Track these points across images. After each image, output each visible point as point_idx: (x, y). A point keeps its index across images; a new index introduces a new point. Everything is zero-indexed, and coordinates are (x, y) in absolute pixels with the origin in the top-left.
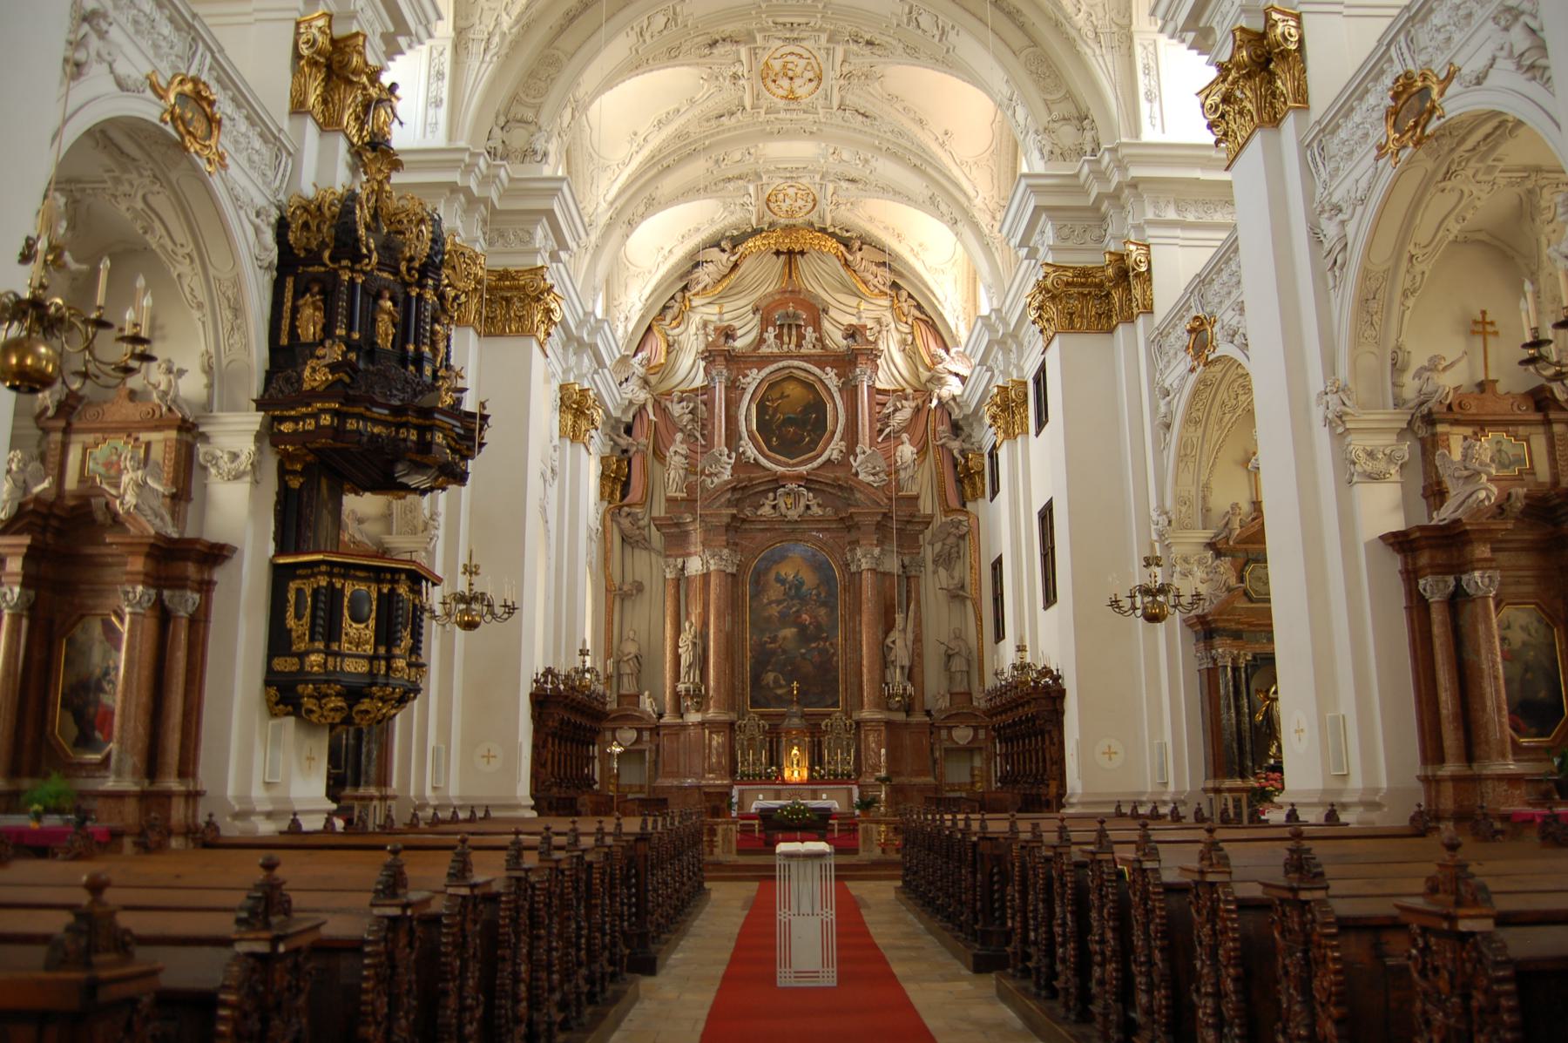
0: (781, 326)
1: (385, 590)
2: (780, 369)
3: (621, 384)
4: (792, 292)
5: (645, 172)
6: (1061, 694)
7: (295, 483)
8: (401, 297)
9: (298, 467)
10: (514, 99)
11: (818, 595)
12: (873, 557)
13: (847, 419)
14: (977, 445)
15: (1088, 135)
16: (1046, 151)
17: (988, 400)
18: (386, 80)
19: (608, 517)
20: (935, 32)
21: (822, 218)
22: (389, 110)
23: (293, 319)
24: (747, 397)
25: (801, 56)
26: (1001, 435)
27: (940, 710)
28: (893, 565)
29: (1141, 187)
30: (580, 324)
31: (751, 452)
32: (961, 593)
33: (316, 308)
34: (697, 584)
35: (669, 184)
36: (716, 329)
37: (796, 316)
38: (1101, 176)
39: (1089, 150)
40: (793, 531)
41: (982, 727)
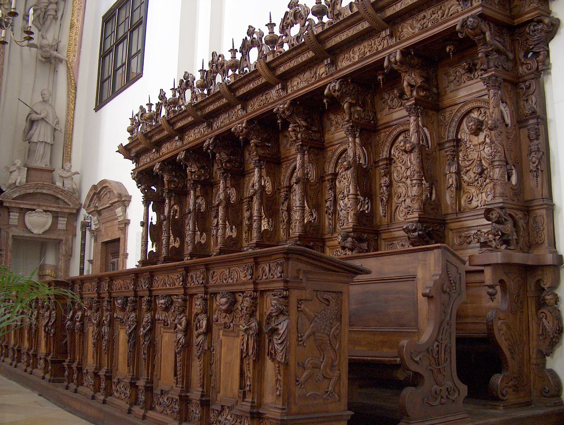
27: (14, 186)
41: (63, 214)
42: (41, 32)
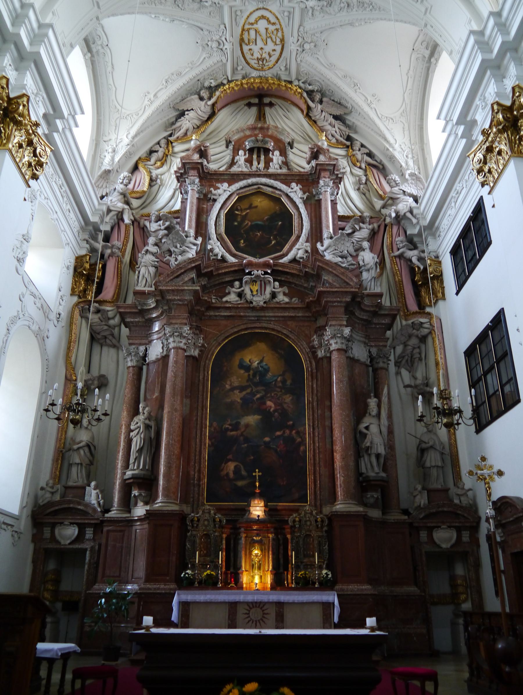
2: (249, 186)
4: (262, 129)
11: (284, 382)
12: (343, 337)
14: (433, 255)
19: (77, 312)
21: (287, 69)
24: (217, 206)
31: (219, 250)
32: (428, 389)
34: (153, 369)
40: (259, 319)
42: (411, 373)
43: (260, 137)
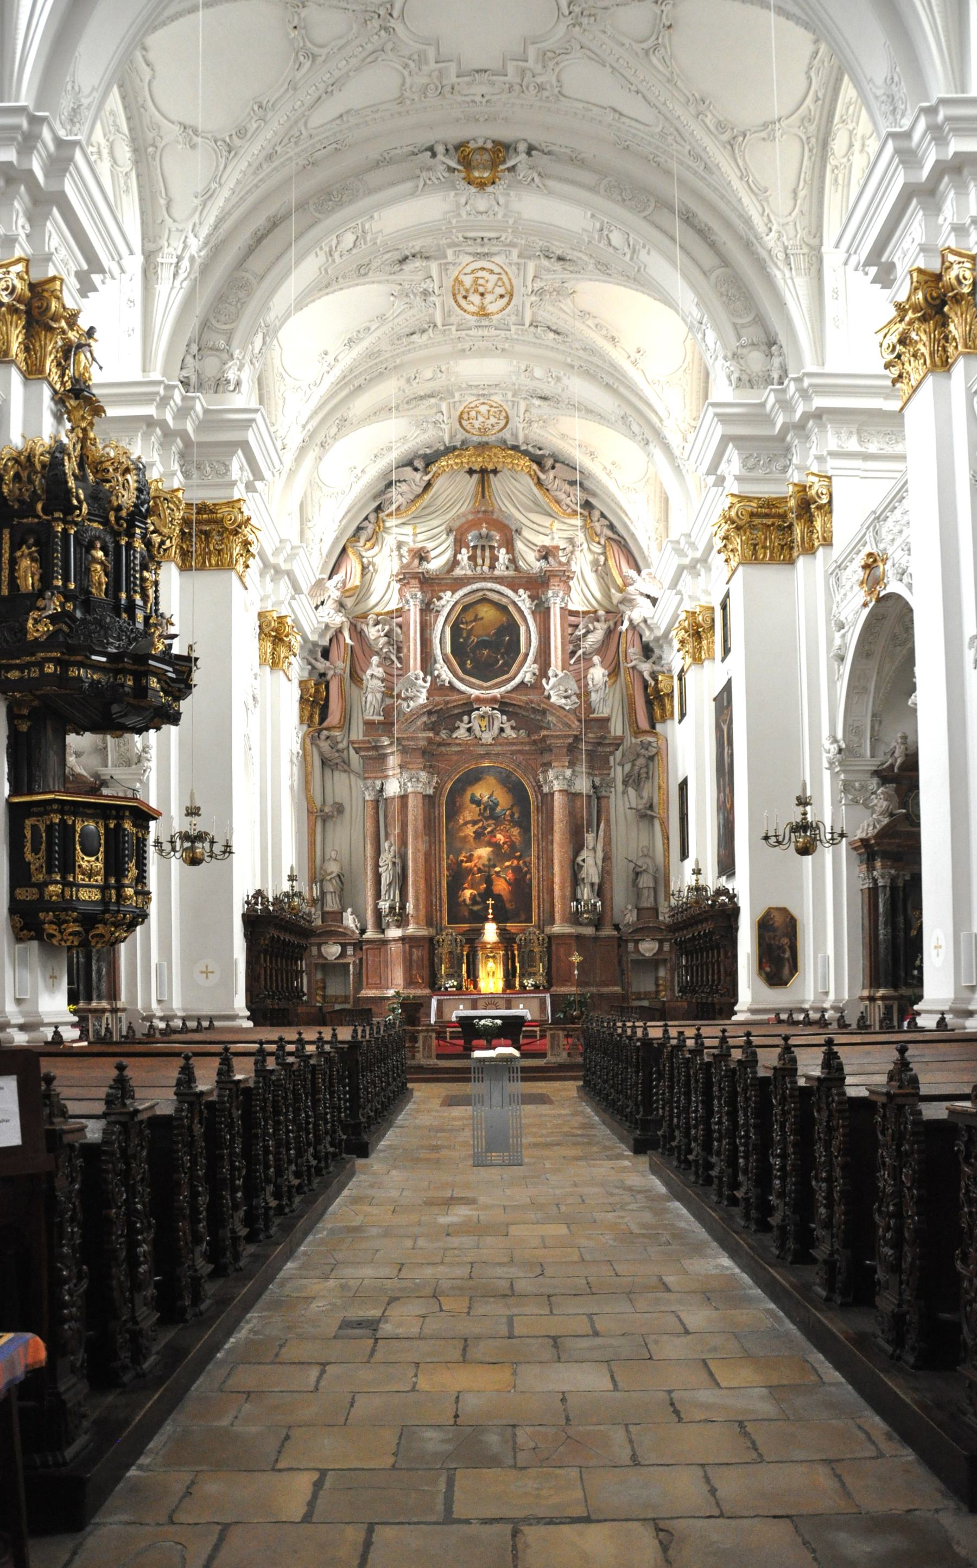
0: (475, 547)
1: (112, 826)
3: (317, 608)
4: (485, 512)
5: (336, 393)
6: (736, 911)
7: (24, 728)
8: (111, 546)
9: (25, 712)
10: (205, 325)
11: (512, 815)
12: (564, 778)
13: (540, 641)
15: (776, 361)
16: (734, 377)
17: (677, 625)
18: (84, 323)
20: (626, 250)
21: (516, 436)
22: (88, 355)
23: (12, 570)
24: (441, 619)
25: (492, 272)
26: (689, 660)
28: (583, 785)
29: (824, 417)
30: (277, 552)
31: (445, 674)
33: (33, 560)
35: (361, 404)
36: (410, 551)
37: (489, 538)
38: (785, 405)
39: (775, 376)
43: (484, 531)
